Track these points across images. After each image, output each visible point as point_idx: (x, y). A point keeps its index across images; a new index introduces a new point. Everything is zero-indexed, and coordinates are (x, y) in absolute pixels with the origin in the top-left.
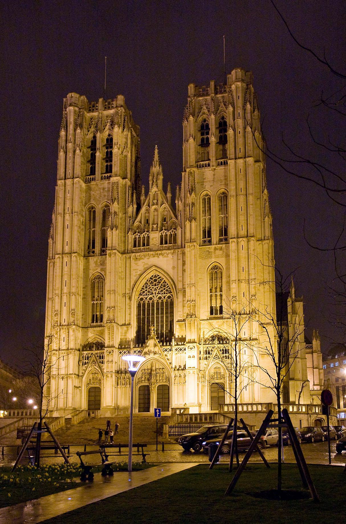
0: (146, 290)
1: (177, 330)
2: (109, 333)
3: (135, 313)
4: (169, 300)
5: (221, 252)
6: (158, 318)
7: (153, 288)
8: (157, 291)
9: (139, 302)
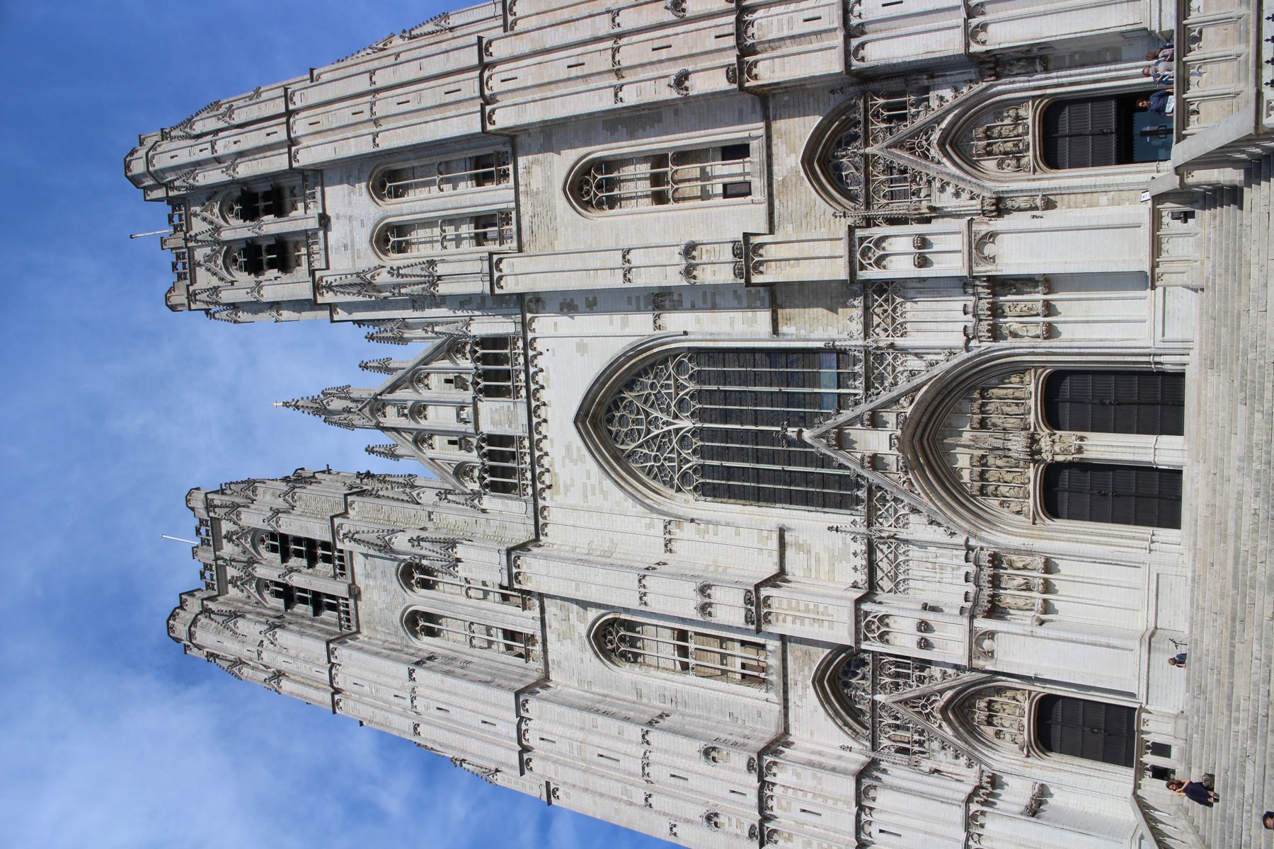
0: (656, 459)
1: (803, 332)
2: (796, 617)
3: (738, 508)
4: (693, 367)
5: (536, 170)
6: (756, 418)
7: (649, 432)
8: (659, 415)
9: (695, 489)
